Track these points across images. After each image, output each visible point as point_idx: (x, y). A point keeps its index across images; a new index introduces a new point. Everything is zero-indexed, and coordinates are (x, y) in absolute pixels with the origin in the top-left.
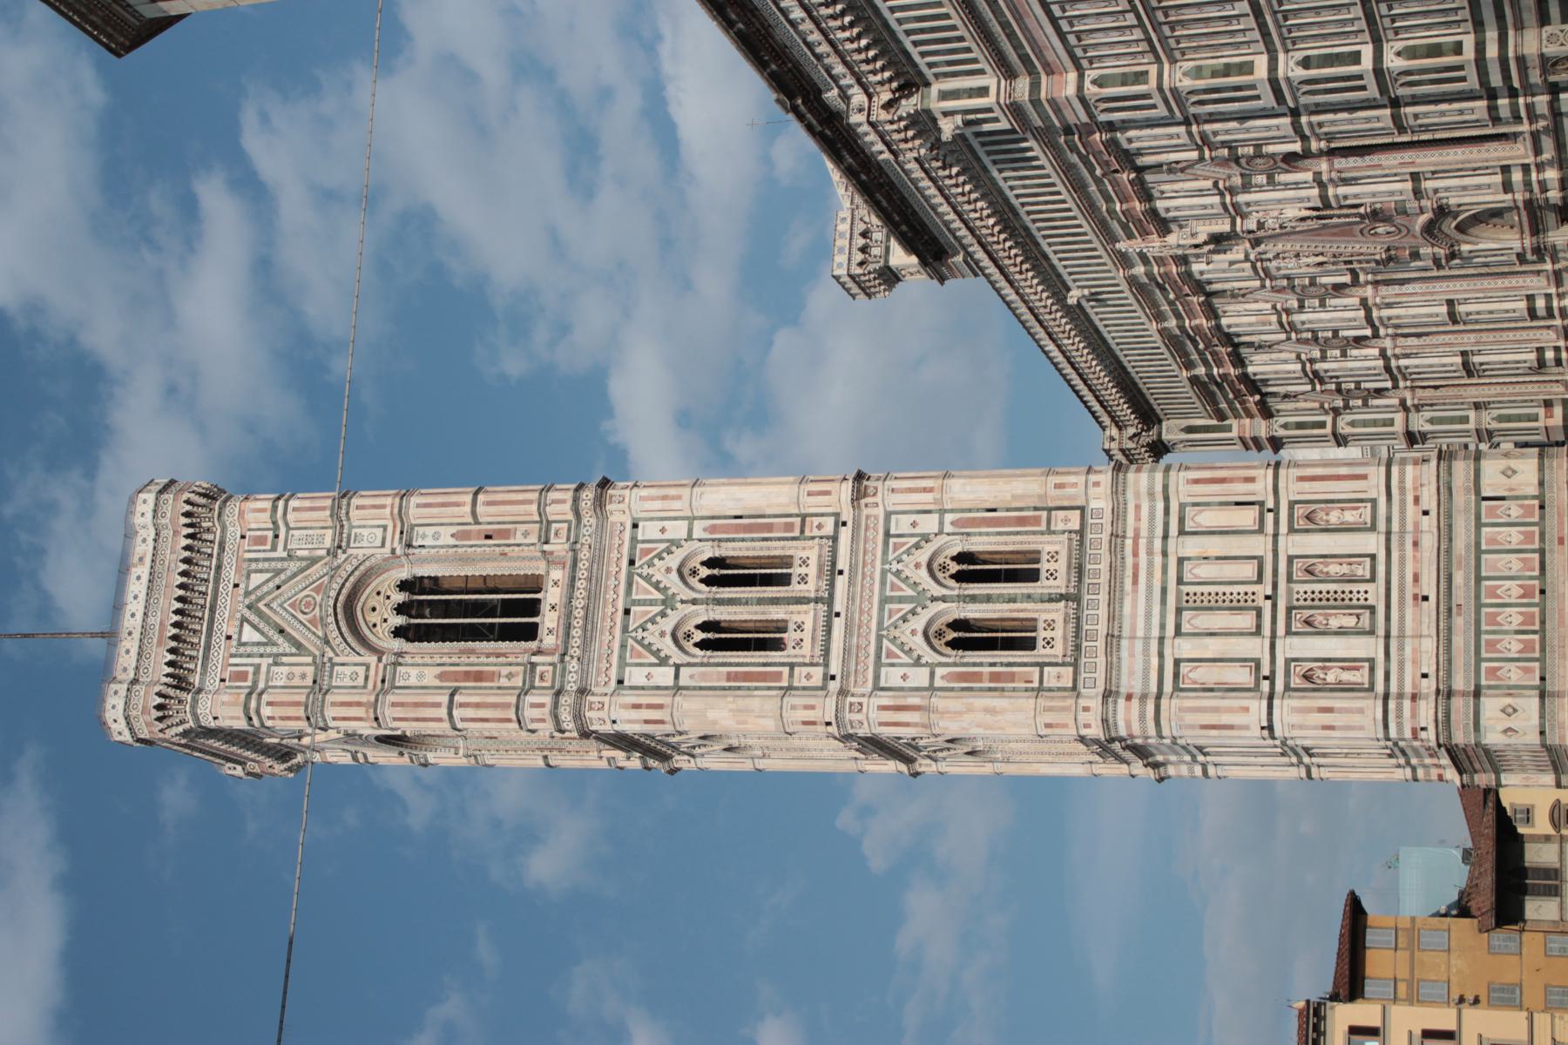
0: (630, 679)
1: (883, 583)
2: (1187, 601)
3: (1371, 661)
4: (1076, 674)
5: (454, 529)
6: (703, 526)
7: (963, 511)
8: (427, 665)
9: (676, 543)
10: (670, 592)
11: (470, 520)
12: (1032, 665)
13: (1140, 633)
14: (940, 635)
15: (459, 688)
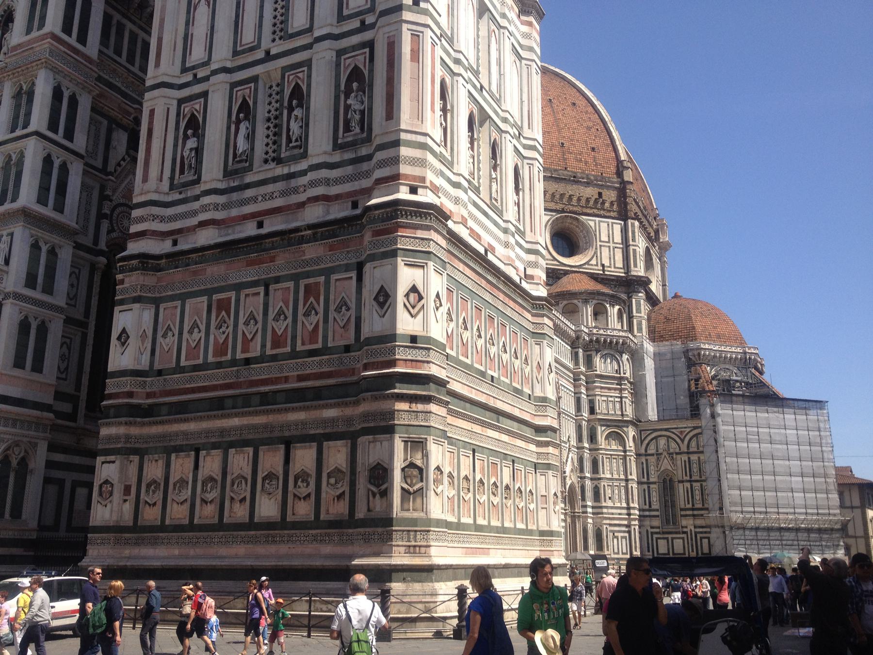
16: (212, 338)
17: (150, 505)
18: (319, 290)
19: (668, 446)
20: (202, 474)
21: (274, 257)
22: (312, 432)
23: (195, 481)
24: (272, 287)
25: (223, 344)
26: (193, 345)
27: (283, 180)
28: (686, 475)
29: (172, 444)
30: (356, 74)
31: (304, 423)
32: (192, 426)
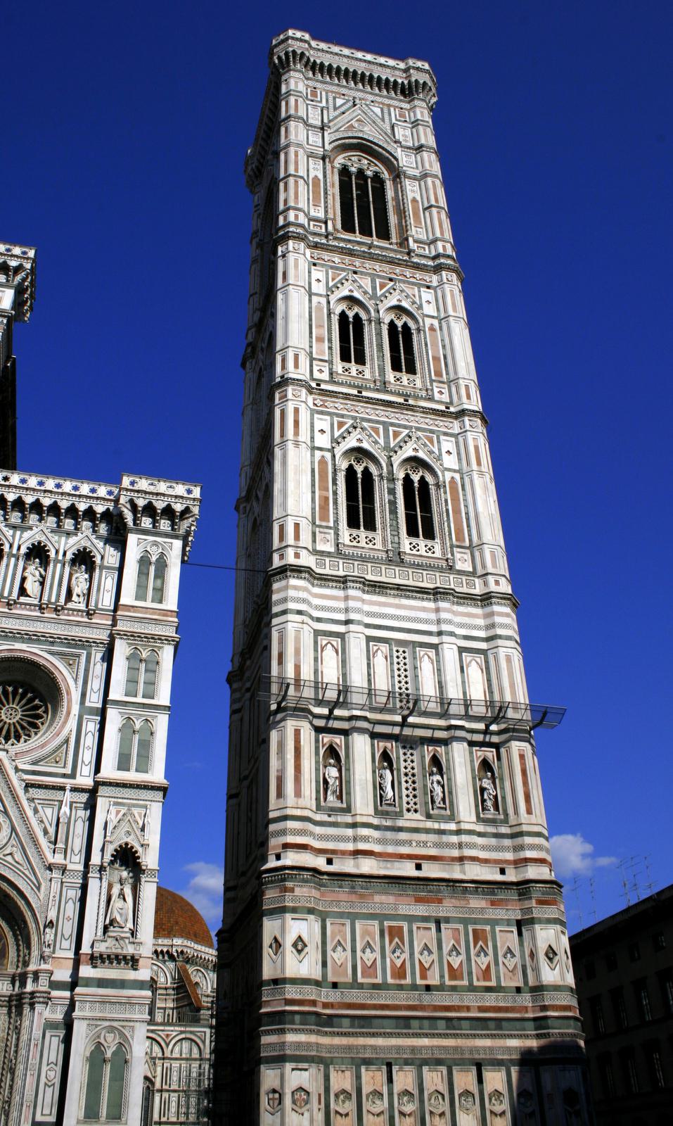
0: (315, 270)
1: (399, 426)
2: (398, 651)
3: (348, 810)
4: (329, 553)
5: (419, 198)
6: (434, 323)
7: (463, 486)
8: (325, 173)
9: (420, 307)
10: (382, 298)
11: (426, 205)
12: (336, 521)
13: (366, 608)
14: (359, 462)
15: (308, 185)
16: (388, 960)
17: (341, 1115)
18: (487, 937)
19: (151, 1049)
20: (397, 1088)
21: (441, 899)
22: (500, 1057)
23: (391, 1094)
24: (443, 926)
25: (400, 967)
26: (369, 964)
27: (435, 834)
28: (166, 1084)
29: (361, 1056)
30: (486, 765)
31: (491, 1049)
32: (380, 1042)
